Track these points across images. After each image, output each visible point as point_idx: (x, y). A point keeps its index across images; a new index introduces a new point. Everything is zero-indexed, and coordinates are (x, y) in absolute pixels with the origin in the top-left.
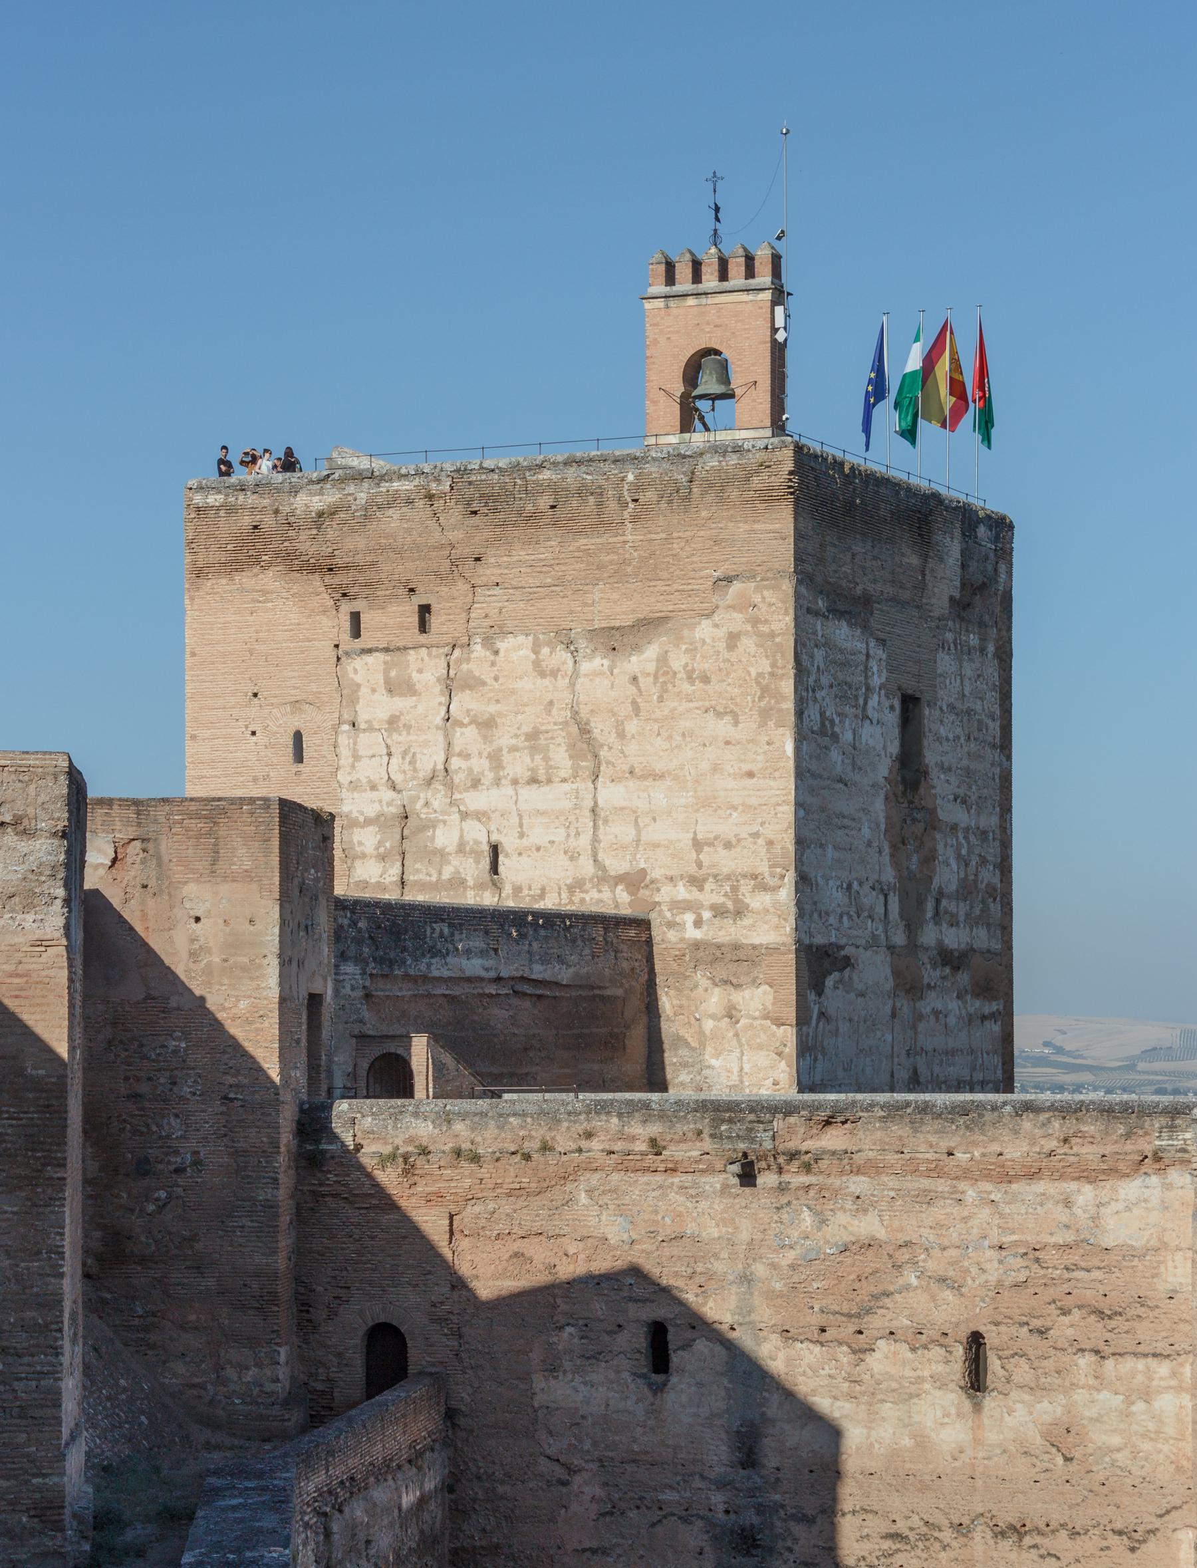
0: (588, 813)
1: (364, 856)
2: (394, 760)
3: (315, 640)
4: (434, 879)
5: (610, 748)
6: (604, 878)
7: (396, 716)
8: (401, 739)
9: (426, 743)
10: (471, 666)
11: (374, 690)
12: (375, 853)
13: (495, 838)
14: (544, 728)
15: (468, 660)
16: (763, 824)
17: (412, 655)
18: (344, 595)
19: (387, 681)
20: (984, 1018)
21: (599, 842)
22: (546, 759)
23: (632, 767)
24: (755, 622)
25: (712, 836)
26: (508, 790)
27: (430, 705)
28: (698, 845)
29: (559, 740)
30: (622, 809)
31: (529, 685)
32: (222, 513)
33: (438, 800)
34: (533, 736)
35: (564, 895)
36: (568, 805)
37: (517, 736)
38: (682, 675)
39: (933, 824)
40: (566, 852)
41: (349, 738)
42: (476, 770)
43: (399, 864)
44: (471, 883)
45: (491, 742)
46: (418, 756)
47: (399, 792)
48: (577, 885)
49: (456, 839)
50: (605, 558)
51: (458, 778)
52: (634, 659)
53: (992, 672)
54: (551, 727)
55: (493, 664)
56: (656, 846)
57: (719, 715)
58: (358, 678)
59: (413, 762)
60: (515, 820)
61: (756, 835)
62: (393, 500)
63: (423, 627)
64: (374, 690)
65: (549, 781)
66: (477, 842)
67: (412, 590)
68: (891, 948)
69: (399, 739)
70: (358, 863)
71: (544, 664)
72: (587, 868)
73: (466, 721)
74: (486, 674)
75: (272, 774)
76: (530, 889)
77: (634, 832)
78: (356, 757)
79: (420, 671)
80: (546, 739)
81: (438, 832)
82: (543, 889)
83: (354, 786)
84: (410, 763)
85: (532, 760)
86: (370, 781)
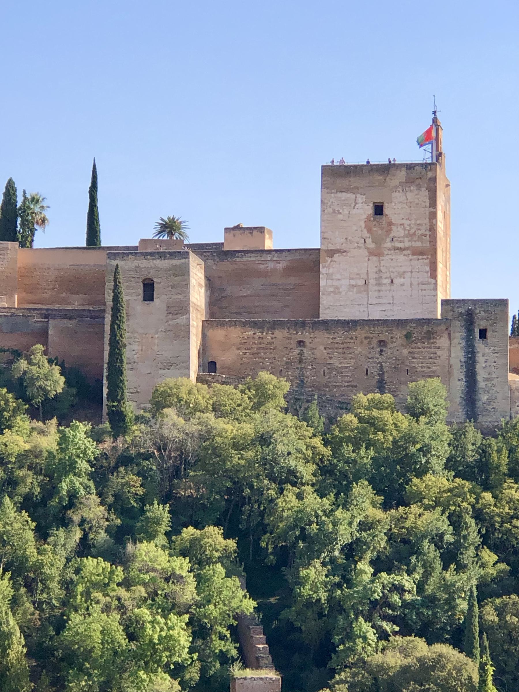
20: (418, 259)
39: (390, 224)
53: (424, 194)
68: (368, 249)
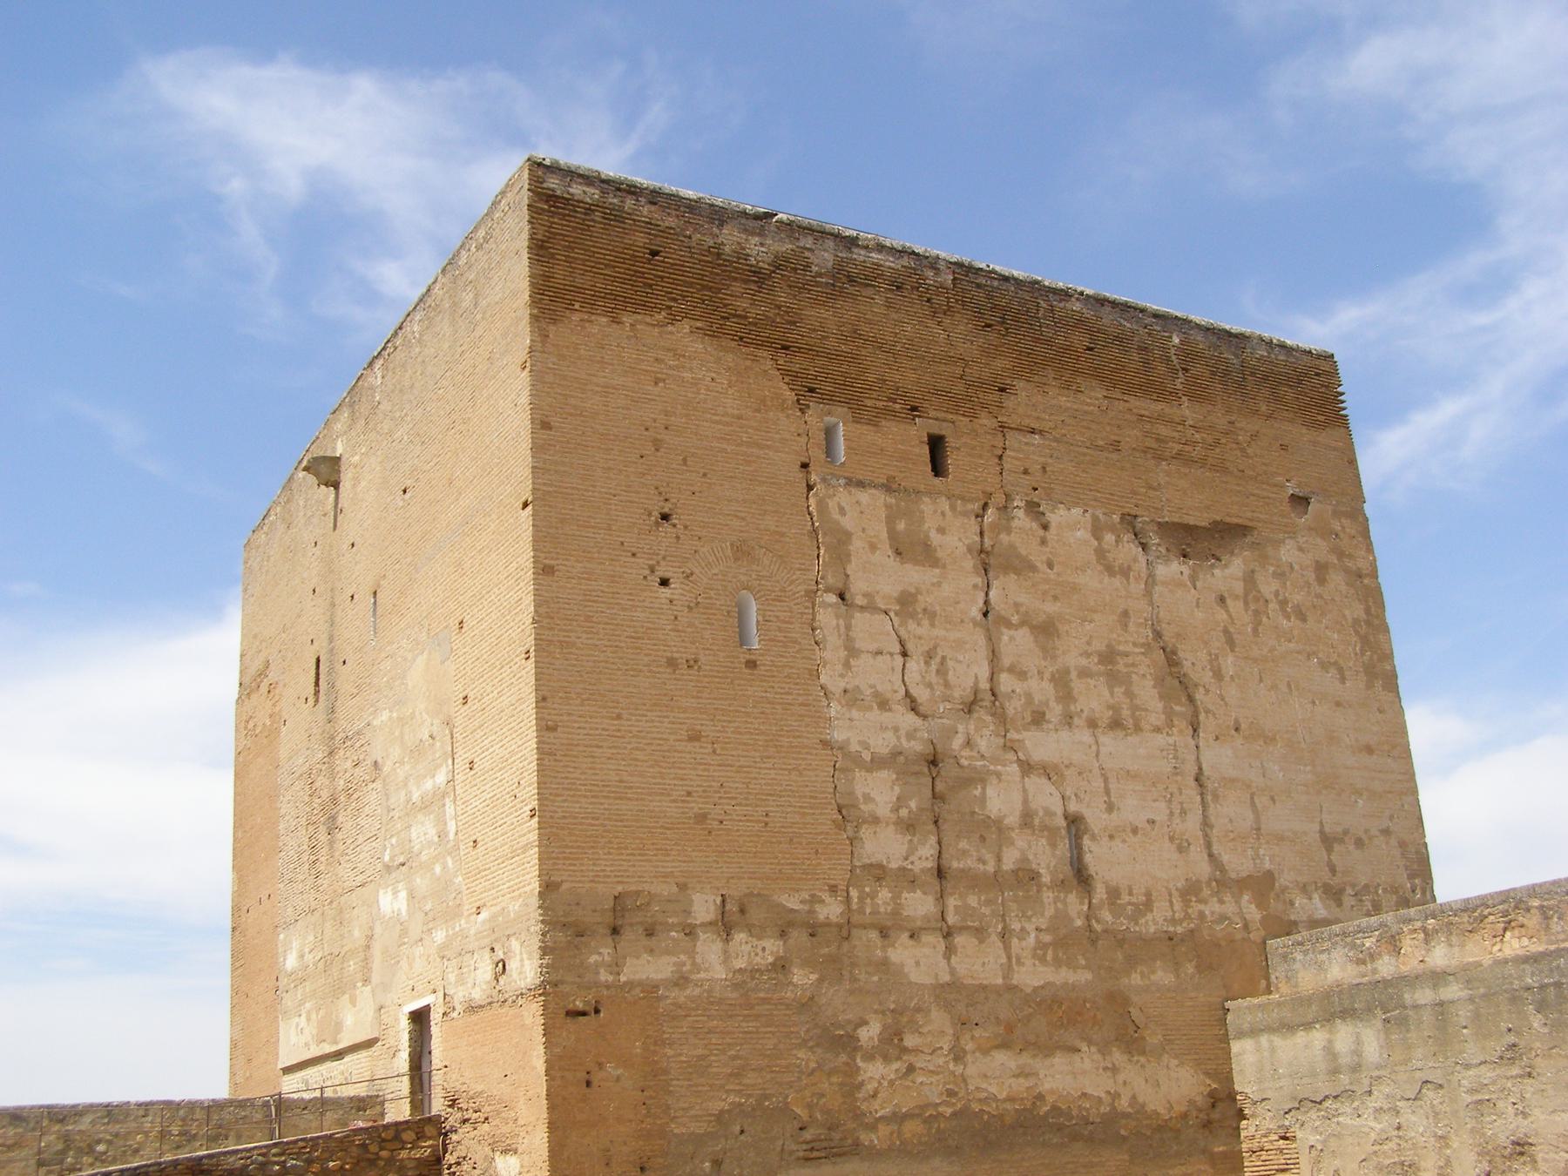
0: (1193, 784)
1: (875, 820)
2: (914, 666)
3: (769, 447)
4: (990, 868)
5: (1207, 691)
6: (1223, 882)
7: (910, 595)
8: (919, 631)
9: (959, 644)
10: (1014, 538)
11: (873, 547)
12: (893, 817)
13: (1073, 807)
14: (1121, 648)
15: (1009, 530)
16: (1391, 818)
17: (926, 505)
18: (812, 390)
19: (893, 535)
21: (1211, 827)
22: (1129, 694)
23: (1237, 721)
24: (1341, 555)
25: (1339, 829)
26: (1085, 736)
27: (956, 586)
28: (1328, 841)
29: (1143, 669)
30: (1233, 780)
31: (1091, 580)
32: (597, 216)
33: (986, 742)
34: (1109, 657)
35: (1177, 906)
36: (1166, 767)
37: (1087, 655)
38: (1273, 606)
40: (1171, 839)
41: (838, 617)
42: (1037, 698)
43: (933, 839)
44: (1046, 879)
45: (1054, 657)
46: (950, 663)
47: (925, 717)
48: (1191, 891)
49: (1019, 806)
50: (1164, 431)
51: (1013, 707)
52: (1217, 572)
54: (1129, 648)
55: (1043, 542)
56: (1281, 838)
57: (1324, 666)
58: (847, 522)
59: (942, 671)
60: (1098, 783)
61: (1386, 832)
62: (871, 277)
63: (938, 468)
64: (873, 547)
65: (1138, 728)
66: (1049, 813)
67: (914, 409)
69: (920, 633)
70: (865, 832)
71: (1110, 556)
72: (1203, 869)
73: (1015, 619)
74: (1037, 557)
75: (702, 659)
76: (1130, 894)
77: (1250, 816)
78: (852, 651)
79: (941, 530)
80: (1126, 665)
81: (990, 792)
82: (1148, 895)
83: (851, 697)
84: (938, 671)
85: (1112, 694)
86: (876, 694)
